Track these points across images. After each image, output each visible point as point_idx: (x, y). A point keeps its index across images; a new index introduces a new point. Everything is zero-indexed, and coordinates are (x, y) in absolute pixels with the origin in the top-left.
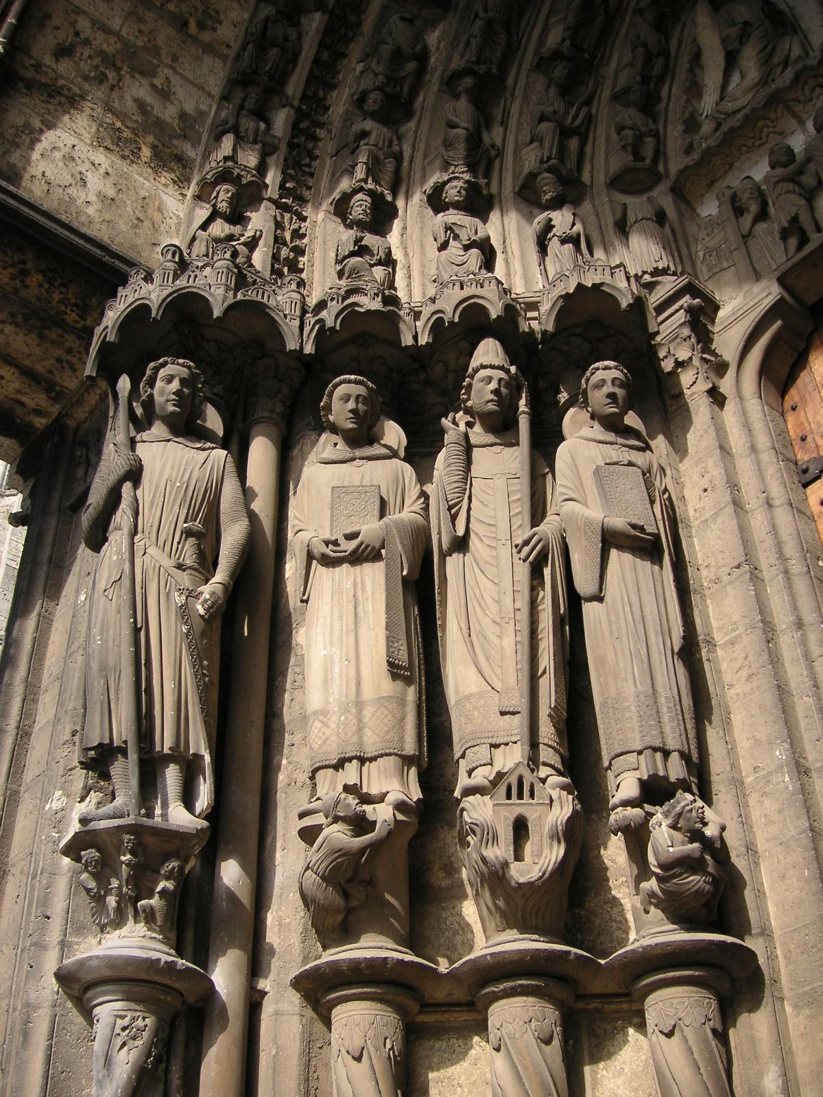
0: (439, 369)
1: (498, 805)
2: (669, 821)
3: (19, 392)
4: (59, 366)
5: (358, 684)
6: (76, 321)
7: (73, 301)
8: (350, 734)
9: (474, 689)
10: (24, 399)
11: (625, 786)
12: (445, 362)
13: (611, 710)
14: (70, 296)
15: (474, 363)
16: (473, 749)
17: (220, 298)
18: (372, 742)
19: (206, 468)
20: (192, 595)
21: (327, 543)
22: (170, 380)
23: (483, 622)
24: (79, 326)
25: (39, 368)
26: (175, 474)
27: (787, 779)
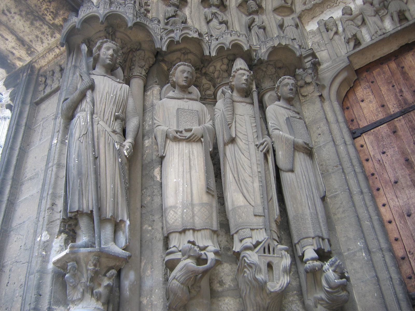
0: (211, 69)
1: (260, 256)
2: (333, 268)
3: (13, 48)
4: (37, 39)
5: (192, 196)
6: (50, 20)
7: (52, 10)
8: (189, 218)
9: (242, 204)
10: (14, 51)
11: (310, 253)
12: (215, 66)
13: (300, 219)
14: (51, 7)
15: (234, 68)
16: (243, 230)
17: (131, 19)
18: (198, 222)
19: (122, 91)
20: (122, 146)
21: (177, 132)
22: (108, 49)
23: (245, 175)
24: (51, 22)
25: (26, 39)
26: (110, 91)
27: (364, 255)
